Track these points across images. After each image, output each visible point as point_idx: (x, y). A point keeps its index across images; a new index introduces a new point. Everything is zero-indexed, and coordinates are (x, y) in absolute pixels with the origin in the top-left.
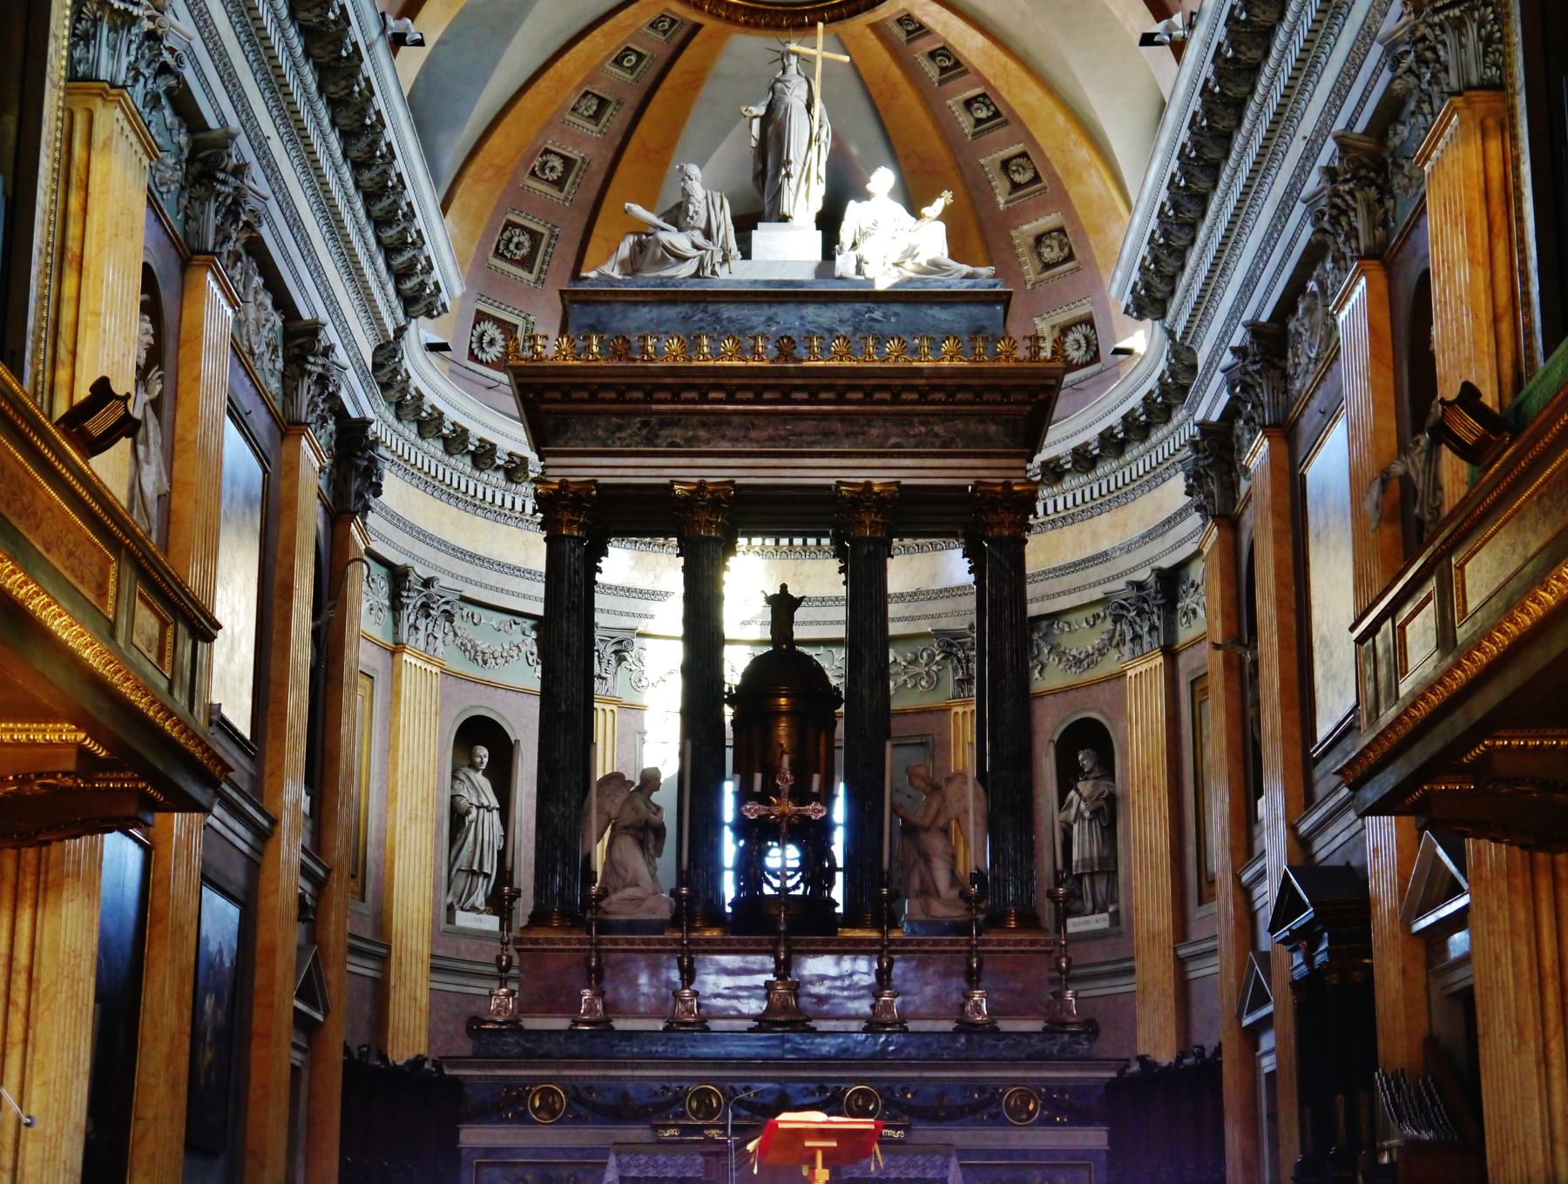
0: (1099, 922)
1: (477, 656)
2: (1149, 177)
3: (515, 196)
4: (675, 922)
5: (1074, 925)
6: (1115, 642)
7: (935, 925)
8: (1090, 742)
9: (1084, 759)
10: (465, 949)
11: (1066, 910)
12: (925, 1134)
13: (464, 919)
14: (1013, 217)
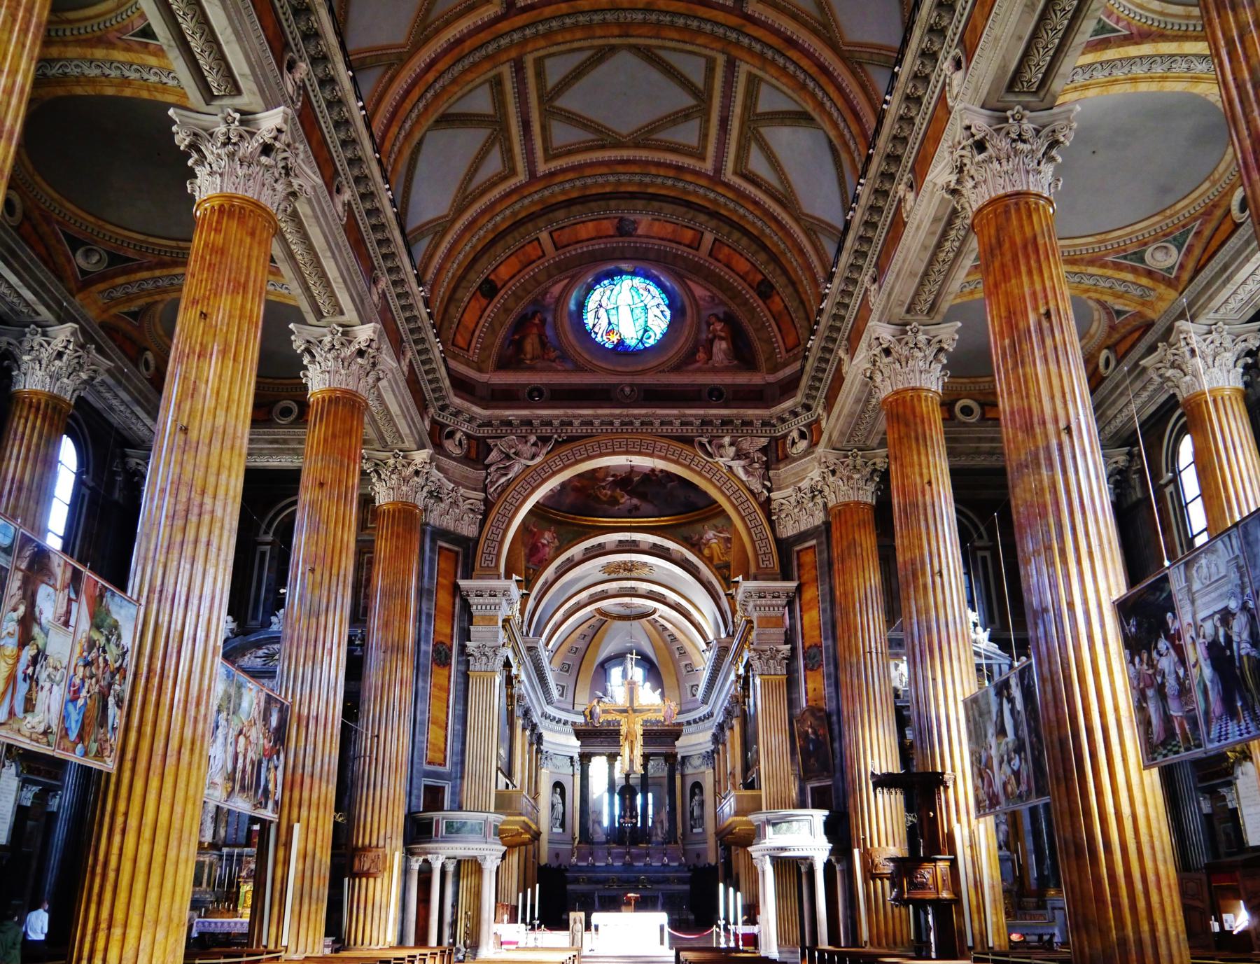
0: (700, 830)
3: (566, 658)
4: (607, 842)
5: (695, 831)
7: (658, 843)
8: (697, 786)
9: (697, 791)
10: (556, 837)
11: (692, 827)
12: (656, 886)
13: (555, 830)
14: (679, 661)
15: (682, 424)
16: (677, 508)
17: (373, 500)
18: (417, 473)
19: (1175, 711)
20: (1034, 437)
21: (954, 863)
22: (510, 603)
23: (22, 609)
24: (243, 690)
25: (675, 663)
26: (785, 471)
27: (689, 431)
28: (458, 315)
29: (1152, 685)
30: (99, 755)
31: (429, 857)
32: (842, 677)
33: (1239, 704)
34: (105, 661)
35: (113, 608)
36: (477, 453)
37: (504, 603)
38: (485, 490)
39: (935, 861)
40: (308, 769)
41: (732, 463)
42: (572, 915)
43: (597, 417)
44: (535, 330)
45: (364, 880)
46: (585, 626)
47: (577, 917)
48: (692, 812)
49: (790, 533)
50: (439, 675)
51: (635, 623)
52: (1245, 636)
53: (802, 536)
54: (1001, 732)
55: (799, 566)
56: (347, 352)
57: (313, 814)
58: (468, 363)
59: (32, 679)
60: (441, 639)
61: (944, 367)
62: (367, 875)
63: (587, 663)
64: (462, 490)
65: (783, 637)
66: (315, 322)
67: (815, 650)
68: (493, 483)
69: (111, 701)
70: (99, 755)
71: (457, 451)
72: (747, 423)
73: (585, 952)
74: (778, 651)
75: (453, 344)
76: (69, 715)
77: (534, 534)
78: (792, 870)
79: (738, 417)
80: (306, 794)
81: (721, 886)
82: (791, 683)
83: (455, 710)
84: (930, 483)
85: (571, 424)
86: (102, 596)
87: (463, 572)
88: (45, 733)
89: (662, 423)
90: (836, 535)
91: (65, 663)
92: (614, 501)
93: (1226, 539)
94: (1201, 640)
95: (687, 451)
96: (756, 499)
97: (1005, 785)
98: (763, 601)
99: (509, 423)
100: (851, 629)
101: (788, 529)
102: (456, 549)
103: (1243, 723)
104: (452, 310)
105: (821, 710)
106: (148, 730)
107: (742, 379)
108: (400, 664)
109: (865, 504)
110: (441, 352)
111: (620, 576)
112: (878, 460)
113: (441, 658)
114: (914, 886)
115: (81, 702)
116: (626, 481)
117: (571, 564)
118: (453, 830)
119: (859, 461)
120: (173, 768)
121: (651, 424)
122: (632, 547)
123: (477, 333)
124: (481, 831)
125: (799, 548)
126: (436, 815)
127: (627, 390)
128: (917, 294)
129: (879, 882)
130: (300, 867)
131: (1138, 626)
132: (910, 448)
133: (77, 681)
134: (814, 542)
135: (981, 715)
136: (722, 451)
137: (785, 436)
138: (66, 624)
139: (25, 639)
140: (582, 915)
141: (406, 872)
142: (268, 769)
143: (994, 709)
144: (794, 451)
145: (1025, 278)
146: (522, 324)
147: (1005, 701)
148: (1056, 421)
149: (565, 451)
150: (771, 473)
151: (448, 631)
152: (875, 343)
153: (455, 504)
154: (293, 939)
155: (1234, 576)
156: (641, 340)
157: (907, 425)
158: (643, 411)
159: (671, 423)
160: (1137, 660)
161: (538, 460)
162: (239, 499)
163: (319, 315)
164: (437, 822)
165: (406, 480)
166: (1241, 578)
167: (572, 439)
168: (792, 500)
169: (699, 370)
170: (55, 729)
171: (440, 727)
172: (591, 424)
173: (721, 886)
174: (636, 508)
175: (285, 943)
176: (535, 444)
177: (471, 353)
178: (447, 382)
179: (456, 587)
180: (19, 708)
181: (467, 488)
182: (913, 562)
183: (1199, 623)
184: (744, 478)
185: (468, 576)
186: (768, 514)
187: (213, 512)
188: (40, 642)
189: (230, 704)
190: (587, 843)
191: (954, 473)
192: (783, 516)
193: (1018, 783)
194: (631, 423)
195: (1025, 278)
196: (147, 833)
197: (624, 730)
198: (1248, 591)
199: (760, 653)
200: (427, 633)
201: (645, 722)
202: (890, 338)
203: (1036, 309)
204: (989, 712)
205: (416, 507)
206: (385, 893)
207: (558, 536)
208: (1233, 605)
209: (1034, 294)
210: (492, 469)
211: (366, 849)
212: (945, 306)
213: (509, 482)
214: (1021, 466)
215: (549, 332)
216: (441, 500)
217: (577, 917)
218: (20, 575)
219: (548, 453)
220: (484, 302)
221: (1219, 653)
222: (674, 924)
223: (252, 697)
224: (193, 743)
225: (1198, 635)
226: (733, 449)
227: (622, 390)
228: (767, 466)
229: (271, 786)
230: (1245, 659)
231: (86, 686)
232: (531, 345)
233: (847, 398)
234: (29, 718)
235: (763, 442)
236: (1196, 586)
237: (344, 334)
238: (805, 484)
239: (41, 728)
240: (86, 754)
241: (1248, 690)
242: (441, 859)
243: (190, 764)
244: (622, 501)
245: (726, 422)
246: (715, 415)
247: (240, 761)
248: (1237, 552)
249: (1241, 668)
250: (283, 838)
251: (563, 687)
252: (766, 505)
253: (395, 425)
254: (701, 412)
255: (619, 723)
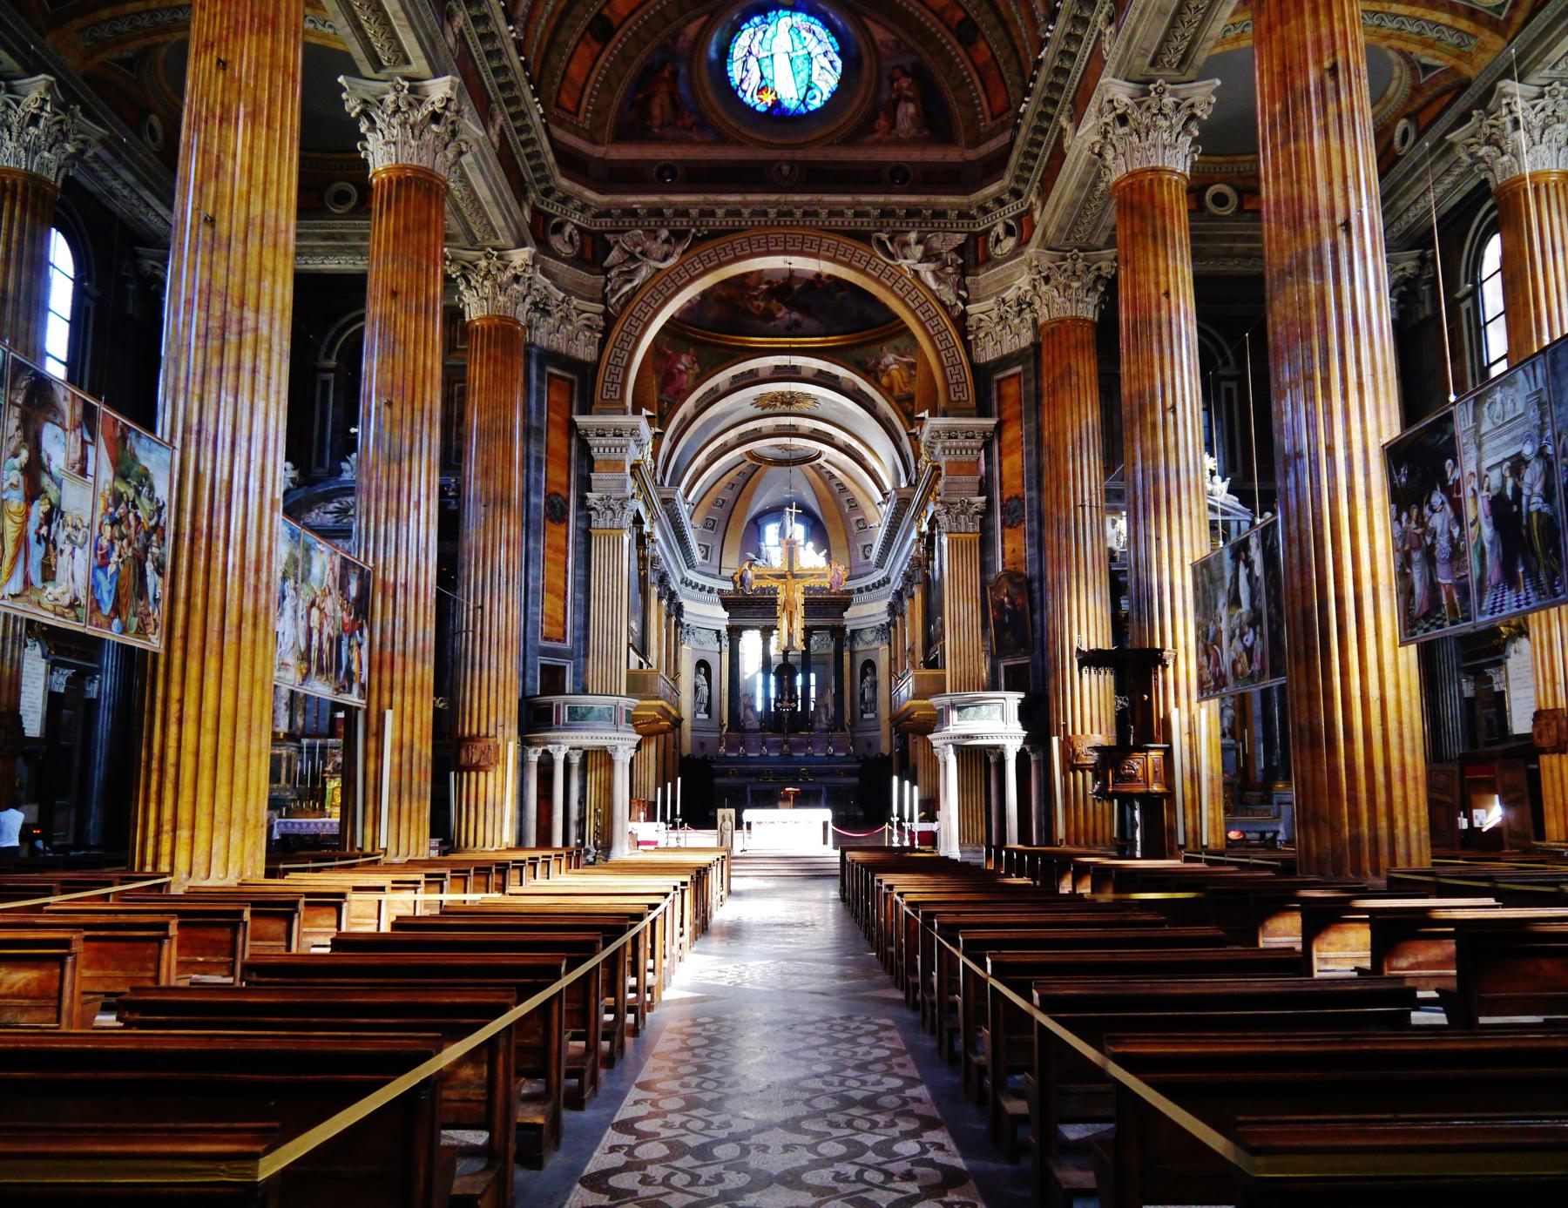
0: (871, 716)
1: (701, 643)
2: (880, 534)
3: (710, 512)
4: (762, 730)
6: (876, 639)
7: (821, 730)
8: (870, 666)
10: (700, 724)
11: (863, 712)
12: (819, 780)
14: (848, 516)
15: (856, 215)
16: (848, 325)
17: (461, 313)
18: (516, 278)
19: (1444, 579)
20: (1303, 235)
21: (1168, 753)
22: (640, 445)
23: (24, 454)
24: (313, 553)
25: (845, 519)
26: (985, 277)
27: (864, 224)
28: (562, 65)
29: (1419, 547)
30: (141, 631)
31: (550, 747)
32: (1047, 536)
33: (1521, 570)
34: (137, 518)
35: (140, 453)
36: (592, 251)
37: (632, 444)
38: (604, 301)
39: (1147, 750)
40: (399, 647)
41: (919, 267)
42: (720, 812)
43: (746, 204)
44: (664, 88)
45: (473, 774)
46: (733, 473)
47: (726, 814)
48: (863, 695)
49: (990, 357)
50: (554, 533)
51: (796, 469)
52: (1538, 488)
53: (1005, 362)
54: (1235, 601)
55: (1000, 399)
56: (417, 116)
57: (408, 699)
58: (577, 132)
59: (48, 541)
60: (554, 489)
61: (1195, 142)
62: (477, 768)
63: (737, 518)
64: (575, 301)
65: (977, 487)
66: (371, 74)
67: (1015, 503)
68: (614, 292)
69: (149, 567)
70: (141, 631)
71: (567, 250)
72: (939, 214)
73: (736, 852)
74: (970, 504)
75: (557, 105)
76: (99, 585)
77: (669, 357)
78: (979, 761)
79: (928, 205)
80: (398, 676)
81: (895, 779)
82: (986, 543)
83: (575, 575)
84: (1167, 294)
85: (713, 214)
86: (124, 438)
87: (579, 406)
88: (73, 605)
89: (831, 214)
90: (1047, 359)
91: (87, 521)
92: (769, 316)
93: (1529, 368)
94: (1485, 493)
95: (862, 251)
96: (948, 314)
97: (1234, 663)
98: (954, 443)
99: (632, 213)
100: (1061, 478)
101: (988, 352)
102: (569, 376)
103: (1523, 593)
104: (554, 58)
105: (1020, 575)
106: (199, 601)
107: (934, 155)
108: (505, 519)
109: (1085, 320)
110: (542, 116)
111: (777, 410)
112: (1103, 264)
113: (557, 512)
114: (1121, 778)
115: (112, 568)
116: (785, 288)
117: (715, 396)
118: (578, 717)
119: (1080, 265)
120: (234, 647)
121: (816, 214)
122: (791, 374)
123: (588, 89)
124: (611, 718)
125: (1000, 376)
126: (556, 699)
127: (785, 168)
128: (1166, 39)
129: (1080, 774)
130: (396, 760)
131: (1410, 476)
132: (1145, 249)
133: (104, 542)
134: (1019, 369)
135: (1212, 581)
136: (907, 251)
137: (987, 232)
138: (83, 472)
139: (33, 492)
140: (732, 811)
141: (523, 765)
142: (350, 647)
143: (1228, 574)
144: (998, 251)
145: (1308, 19)
146: (646, 79)
147: (1242, 565)
148: (1332, 215)
149: (706, 249)
150: (968, 280)
151: (564, 479)
152: (1107, 107)
153: (566, 319)
154: (393, 840)
155: (1533, 415)
156: (803, 101)
157: (1143, 219)
158: (806, 198)
159: (842, 214)
160: (1404, 516)
161: (671, 262)
162: (289, 313)
163: (377, 64)
164: (558, 707)
165: (503, 288)
166: (1542, 416)
167: (715, 234)
168: (994, 314)
169: (878, 143)
170: (84, 602)
171: (558, 596)
172: (738, 214)
173: (895, 779)
174: (797, 324)
175: (383, 845)
176: (667, 241)
177: (581, 117)
178: (551, 158)
179: (572, 425)
180: (36, 577)
181: (579, 297)
182: (1141, 395)
183: (1484, 472)
184: (934, 287)
185: (585, 411)
186: (963, 332)
187: (256, 329)
188: (53, 495)
189: (298, 569)
190: (737, 730)
191: (1200, 281)
192: (982, 335)
193: (1250, 662)
194: (791, 214)
195: (1308, 19)
196: (209, 722)
197: (781, 598)
198: (1548, 433)
199: (948, 506)
200: (538, 482)
201: (807, 589)
202: (1127, 100)
203: (1319, 62)
204: (1222, 578)
205: (517, 322)
206: (499, 789)
207: (699, 360)
208: (1528, 450)
209: (1318, 41)
210: (613, 273)
211: (474, 739)
212: (1201, 57)
213: (635, 291)
214: (1285, 273)
215: (683, 89)
216: (549, 314)
217: (726, 814)
218: (17, 410)
219: (684, 252)
220: (596, 47)
221: (1503, 509)
222: (837, 821)
223: (324, 561)
224: (255, 617)
225: (1481, 487)
226: (921, 248)
227: (780, 170)
228: (963, 271)
229: (355, 667)
230: (1535, 517)
231: (117, 548)
232: (659, 108)
233: (1068, 183)
234: (50, 588)
235: (959, 238)
236: (1486, 426)
237: (412, 90)
238: (1010, 295)
239: (66, 600)
240: (124, 630)
241: (1534, 553)
242: (564, 749)
243: (254, 641)
244: (780, 315)
245: (913, 212)
246: (899, 204)
247: (315, 637)
248: (1541, 384)
249: (1529, 527)
250: (373, 727)
251: (707, 547)
252: (961, 321)
253: (485, 215)
254: (881, 199)
255: (775, 590)
